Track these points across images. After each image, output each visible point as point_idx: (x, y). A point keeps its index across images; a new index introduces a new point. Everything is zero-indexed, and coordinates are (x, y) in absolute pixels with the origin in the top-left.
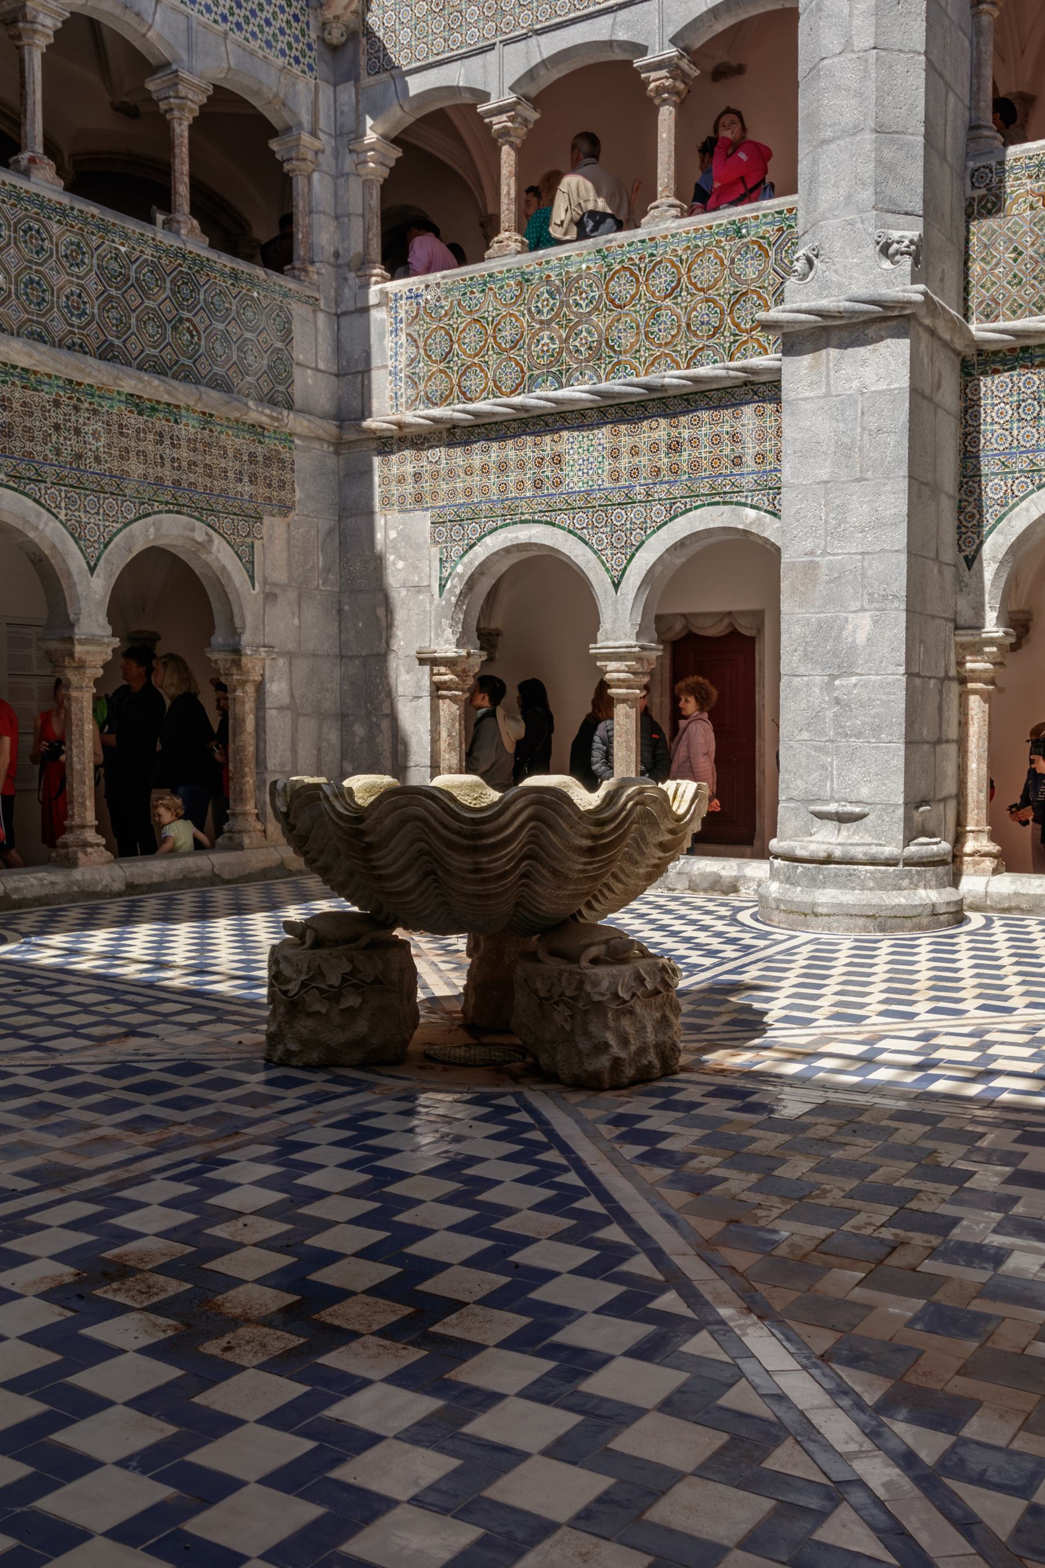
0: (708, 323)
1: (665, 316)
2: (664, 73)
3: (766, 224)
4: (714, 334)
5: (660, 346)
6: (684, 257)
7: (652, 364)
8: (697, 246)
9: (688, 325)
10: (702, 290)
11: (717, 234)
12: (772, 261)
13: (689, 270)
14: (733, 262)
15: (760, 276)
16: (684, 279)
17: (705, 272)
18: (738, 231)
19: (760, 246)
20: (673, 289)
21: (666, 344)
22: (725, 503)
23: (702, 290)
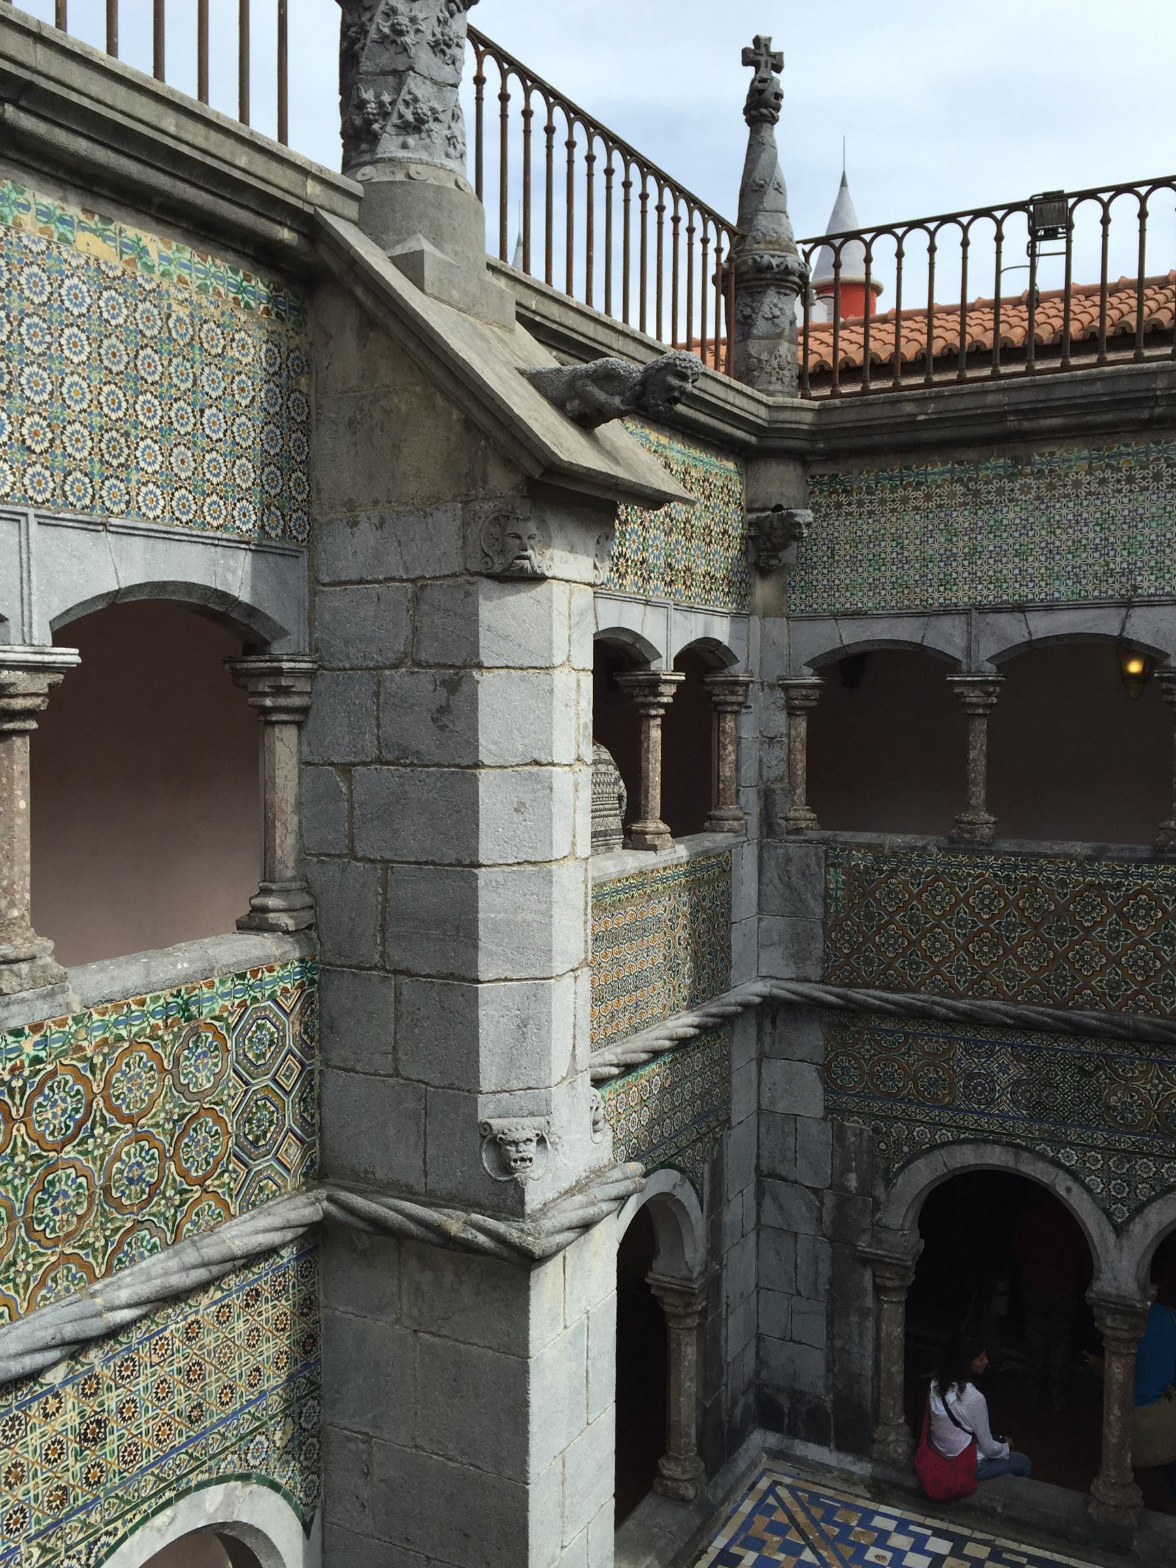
0: (141, 1179)
1: (66, 1182)
2: (41, 683)
3: (223, 996)
4: (150, 1197)
5: (56, 1242)
6: (98, 1060)
7: (42, 1283)
8: (120, 1039)
9: (107, 1190)
10: (129, 1119)
11: (153, 1014)
12: (231, 1057)
13: (107, 1082)
14: (176, 1062)
15: (215, 1086)
16: (99, 1102)
17: (137, 1086)
18: (185, 1007)
19: (216, 1033)
20: (80, 1125)
21: (68, 1235)
22: (180, 1495)
23: (129, 1119)
